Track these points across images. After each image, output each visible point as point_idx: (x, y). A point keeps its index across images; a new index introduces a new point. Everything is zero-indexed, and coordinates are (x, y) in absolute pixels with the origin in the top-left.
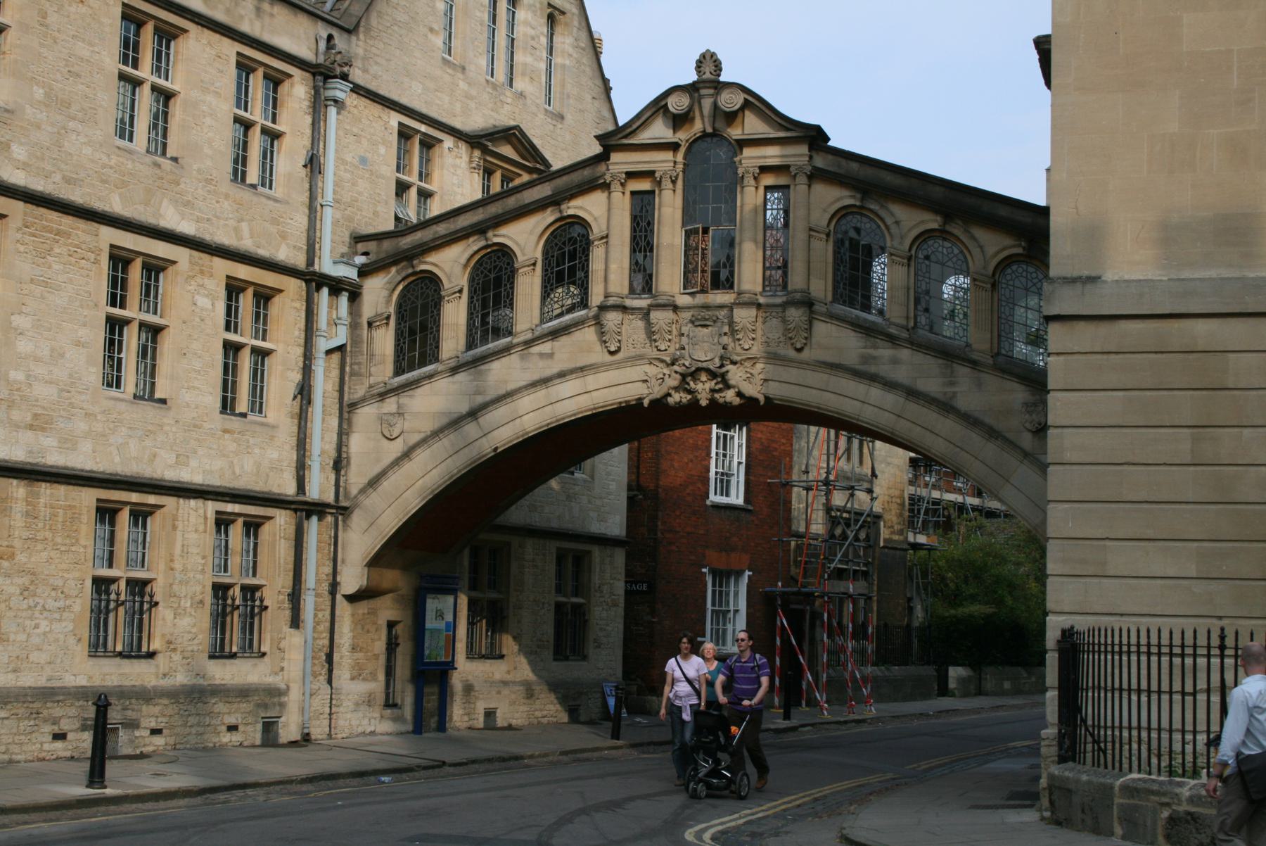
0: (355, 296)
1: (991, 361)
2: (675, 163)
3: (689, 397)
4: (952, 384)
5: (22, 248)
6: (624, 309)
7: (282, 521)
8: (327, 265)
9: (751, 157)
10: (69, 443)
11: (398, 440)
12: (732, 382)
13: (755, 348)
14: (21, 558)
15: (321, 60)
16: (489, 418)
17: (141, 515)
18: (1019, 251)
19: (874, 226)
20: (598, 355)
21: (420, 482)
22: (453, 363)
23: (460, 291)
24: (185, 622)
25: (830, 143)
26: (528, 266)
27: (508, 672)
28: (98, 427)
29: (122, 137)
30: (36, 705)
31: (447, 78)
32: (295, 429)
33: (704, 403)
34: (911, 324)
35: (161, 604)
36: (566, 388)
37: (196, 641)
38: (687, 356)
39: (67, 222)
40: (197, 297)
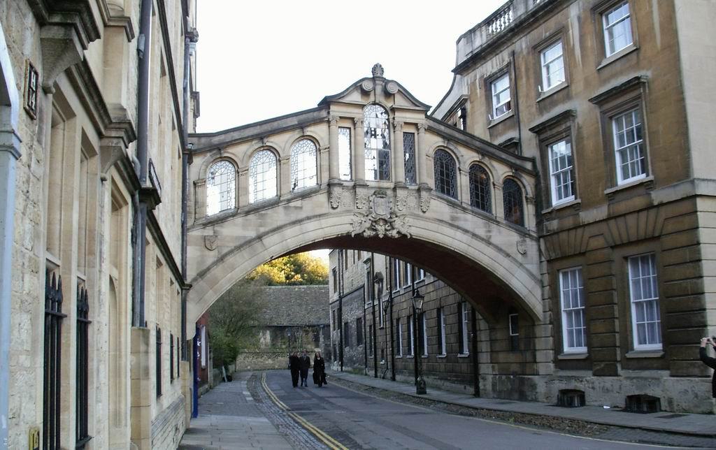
1: (504, 222)
3: (374, 233)
4: (489, 231)
12: (396, 226)
18: (511, 174)
20: (326, 208)
22: (246, 209)
33: (381, 236)
36: (310, 225)
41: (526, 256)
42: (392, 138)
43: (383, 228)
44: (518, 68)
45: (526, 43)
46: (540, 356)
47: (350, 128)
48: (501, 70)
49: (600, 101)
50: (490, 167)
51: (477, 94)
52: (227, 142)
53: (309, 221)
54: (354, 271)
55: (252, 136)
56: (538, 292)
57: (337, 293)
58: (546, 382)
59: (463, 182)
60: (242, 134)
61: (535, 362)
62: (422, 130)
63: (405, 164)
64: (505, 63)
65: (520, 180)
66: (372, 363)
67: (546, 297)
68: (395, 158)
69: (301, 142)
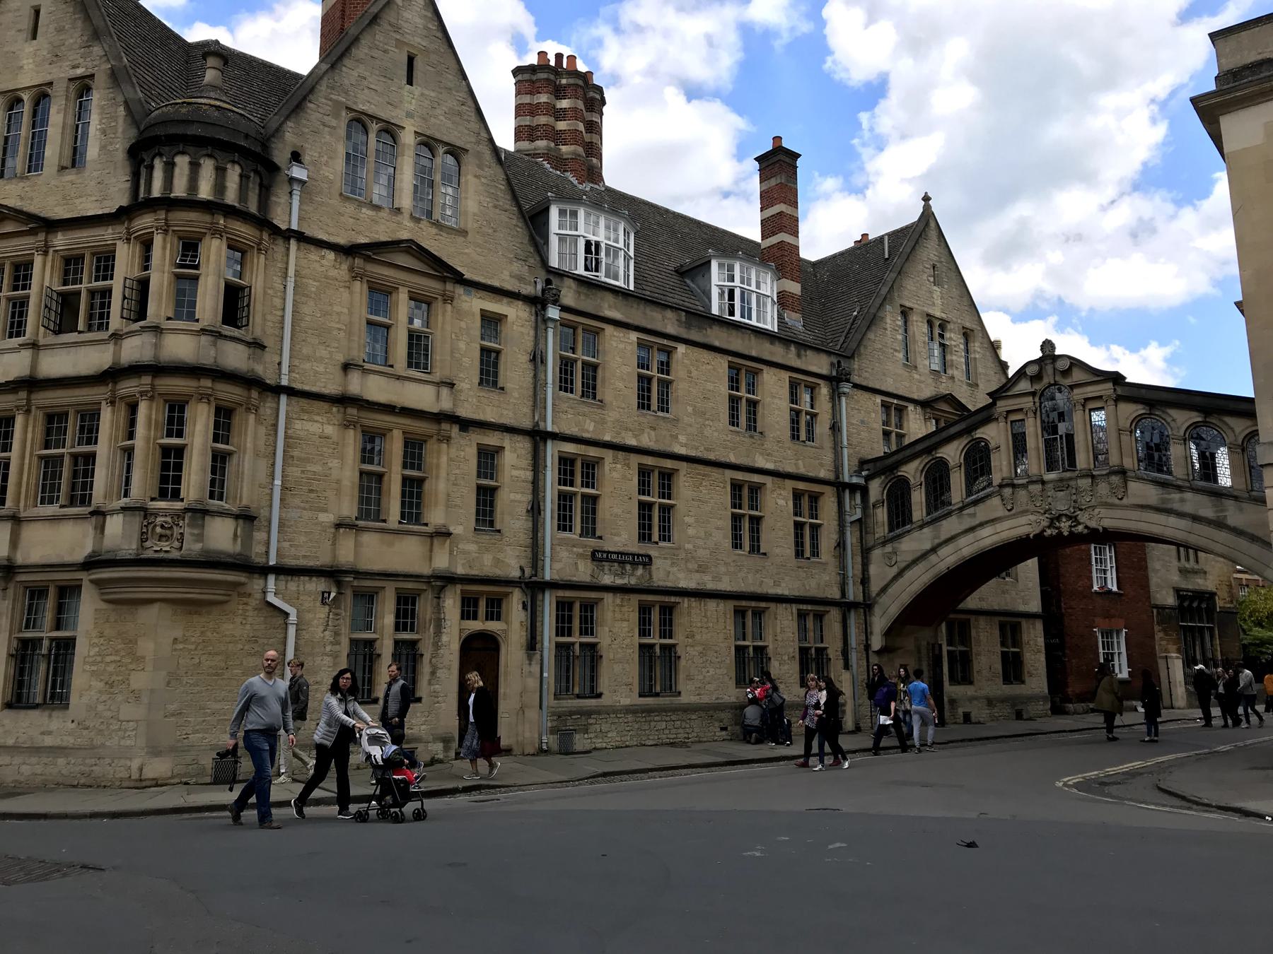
0: (864, 491)
2: (1034, 402)
3: (1057, 531)
4: (1222, 511)
5: (687, 484)
6: (1013, 486)
7: (834, 615)
8: (846, 478)
9: (1079, 394)
10: (717, 578)
12: (1082, 521)
14: (698, 637)
15: (834, 373)
16: (943, 552)
17: (758, 614)
19: (1160, 424)
20: (1001, 512)
22: (920, 523)
24: (786, 667)
25: (1127, 381)
27: (976, 691)
28: (732, 569)
29: (733, 425)
30: (711, 712)
31: (907, 374)
32: (838, 564)
33: (1066, 534)
34: (1191, 478)
35: (772, 659)
37: (793, 677)
39: (708, 469)
40: (778, 500)
47: (1024, 420)
52: (900, 461)
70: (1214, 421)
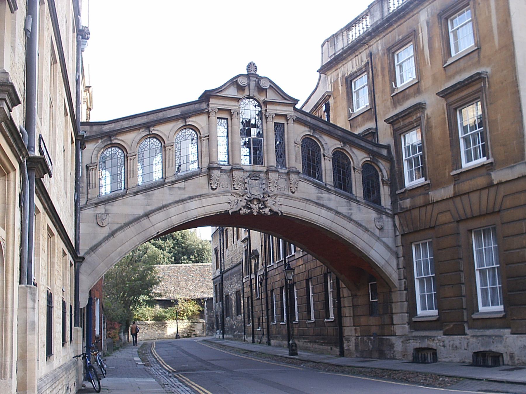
1: (364, 201)
3: (249, 211)
4: (350, 209)
9: (272, 109)
11: (106, 227)
12: (269, 205)
13: (275, 191)
16: (154, 218)
18: (369, 159)
20: (206, 190)
21: (119, 249)
22: (135, 190)
23: (136, 155)
26: (171, 146)
33: (255, 214)
36: (193, 204)
38: (248, 193)
41: (383, 231)
42: (264, 128)
43: (257, 206)
44: (375, 67)
45: (382, 46)
46: (396, 319)
47: (227, 119)
48: (361, 69)
49: (445, 94)
50: (351, 154)
51: (339, 90)
52: (117, 130)
53: (191, 200)
54: (234, 249)
55: (140, 125)
56: (394, 263)
57: (219, 270)
58: (402, 342)
59: (327, 165)
60: (130, 123)
61: (392, 324)
62: (291, 121)
63: (276, 151)
64: (364, 63)
65: (376, 164)
66: (250, 330)
67: (401, 266)
68: (267, 145)
69: (184, 131)
70: (347, 150)
